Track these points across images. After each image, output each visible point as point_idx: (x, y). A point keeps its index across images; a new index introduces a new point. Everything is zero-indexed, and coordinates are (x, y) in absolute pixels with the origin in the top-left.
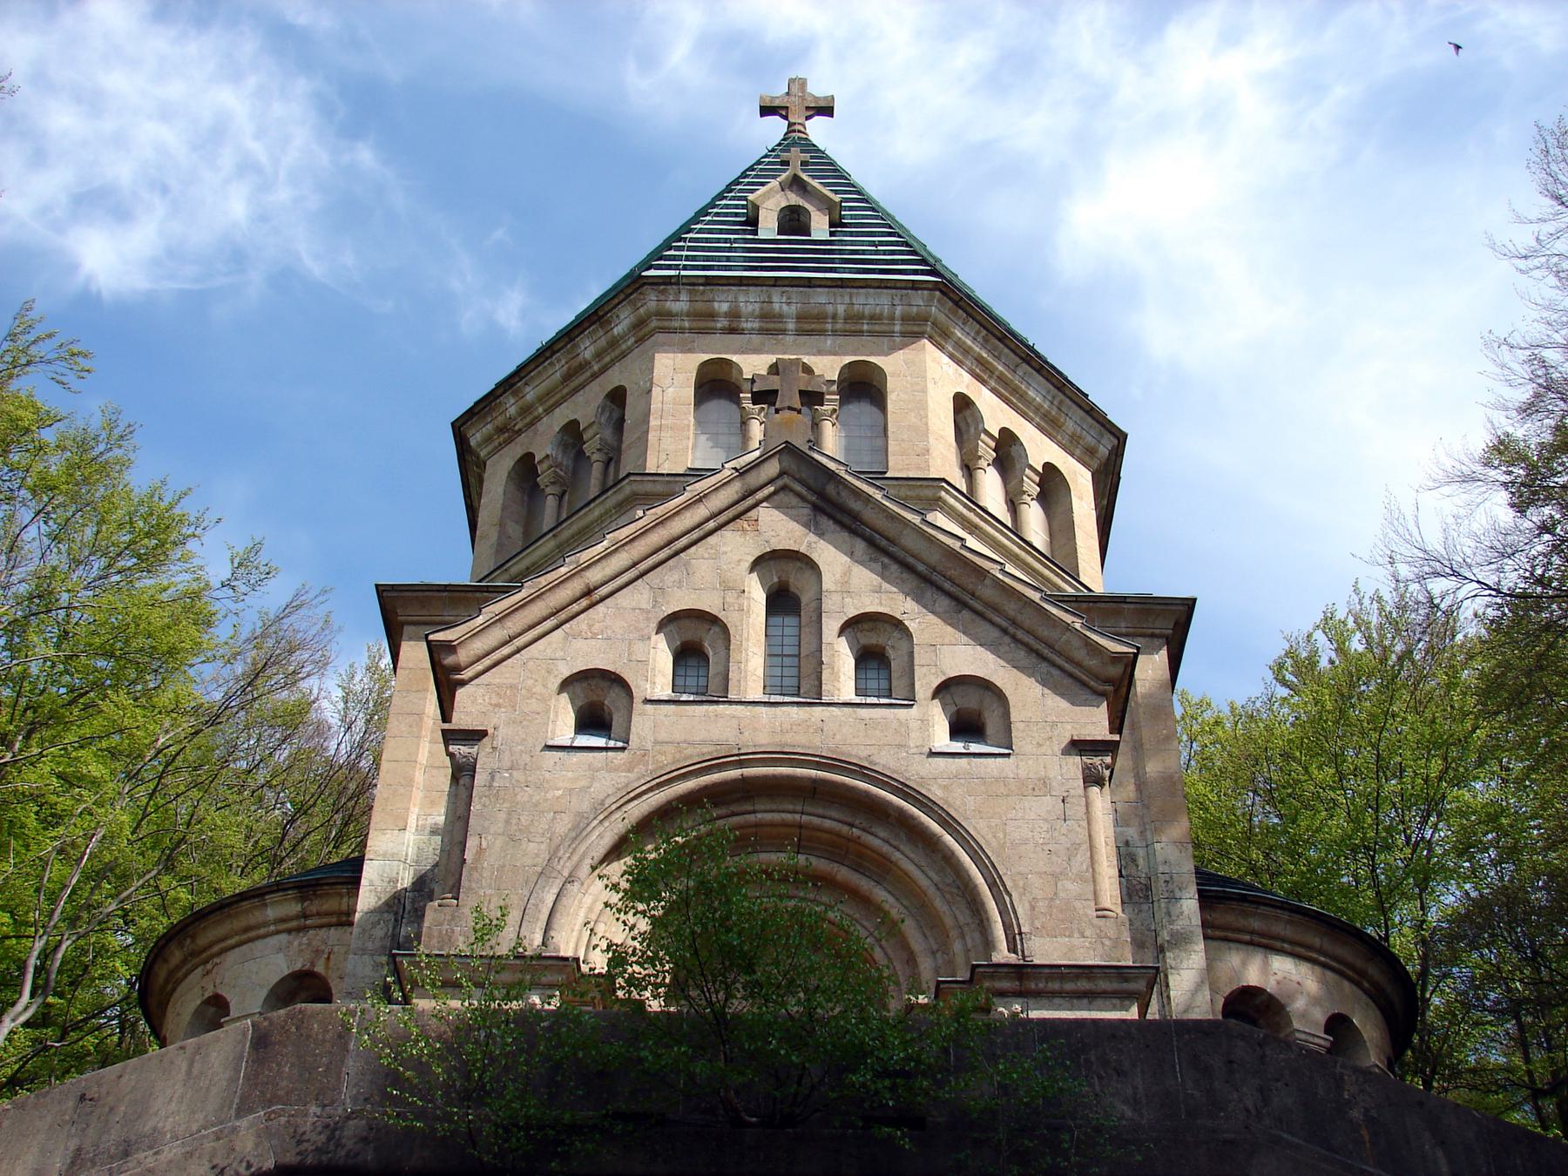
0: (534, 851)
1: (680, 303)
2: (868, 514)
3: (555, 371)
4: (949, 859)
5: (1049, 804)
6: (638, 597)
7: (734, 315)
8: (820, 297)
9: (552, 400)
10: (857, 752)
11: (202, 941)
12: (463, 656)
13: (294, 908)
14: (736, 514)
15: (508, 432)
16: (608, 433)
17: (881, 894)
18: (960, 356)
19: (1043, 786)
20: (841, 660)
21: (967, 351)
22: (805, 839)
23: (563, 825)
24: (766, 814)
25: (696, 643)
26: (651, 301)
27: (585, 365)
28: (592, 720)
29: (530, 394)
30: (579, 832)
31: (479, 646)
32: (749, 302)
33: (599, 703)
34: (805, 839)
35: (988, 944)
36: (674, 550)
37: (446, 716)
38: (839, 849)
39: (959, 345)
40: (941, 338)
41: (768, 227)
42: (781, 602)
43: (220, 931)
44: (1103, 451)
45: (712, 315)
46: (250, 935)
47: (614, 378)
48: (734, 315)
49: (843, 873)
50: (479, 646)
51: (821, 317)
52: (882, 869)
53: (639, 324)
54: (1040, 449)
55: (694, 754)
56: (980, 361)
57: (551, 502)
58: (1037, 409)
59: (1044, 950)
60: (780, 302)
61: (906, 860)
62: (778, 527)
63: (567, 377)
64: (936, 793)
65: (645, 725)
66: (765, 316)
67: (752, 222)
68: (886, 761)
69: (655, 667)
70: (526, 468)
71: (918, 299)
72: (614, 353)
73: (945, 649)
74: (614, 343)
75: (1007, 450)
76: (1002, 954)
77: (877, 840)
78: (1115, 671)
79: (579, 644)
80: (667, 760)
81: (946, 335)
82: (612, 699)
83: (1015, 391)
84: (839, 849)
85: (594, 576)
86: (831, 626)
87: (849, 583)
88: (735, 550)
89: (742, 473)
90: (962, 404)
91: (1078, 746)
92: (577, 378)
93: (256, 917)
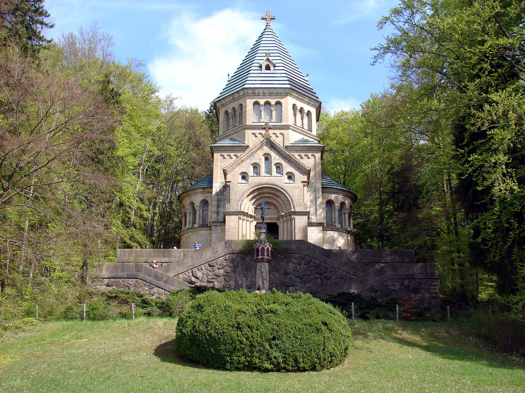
0: (238, 197)
1: (250, 91)
2: (277, 148)
3: (231, 98)
4: (287, 197)
5: (299, 190)
6: (248, 161)
7: (259, 93)
8: (272, 90)
9: (230, 102)
10: (276, 183)
11: (189, 193)
12: (227, 171)
13: (202, 191)
14: (260, 148)
15: (223, 105)
16: (240, 110)
17: (279, 200)
18: (294, 97)
19: (298, 187)
20: (274, 168)
21: (295, 96)
22: (269, 193)
23: (241, 194)
24: (265, 191)
25: (256, 166)
26: (246, 91)
27: (235, 98)
28: (244, 178)
29: (227, 100)
30: (243, 194)
31: (229, 169)
32: (261, 91)
33: (244, 176)
34: (269, 193)
35: (291, 208)
36: (253, 154)
37: (225, 179)
38: (274, 194)
39: (294, 96)
40: (291, 95)
41: (264, 68)
42: (267, 159)
43: (192, 192)
44: (318, 106)
45: (255, 93)
46: (196, 193)
47: (241, 101)
48: (259, 93)
49: (275, 197)
50: (229, 169)
51: (272, 93)
52: (279, 197)
53: (244, 94)
54: (307, 108)
55: (257, 183)
56: (297, 97)
57: (231, 120)
58: (307, 102)
59: (298, 209)
60: (265, 91)
61: (282, 196)
62: (266, 149)
63: (233, 99)
64: (285, 189)
65: (250, 179)
66: (263, 93)
67: (261, 67)
68: (279, 184)
69: (251, 171)
70: (227, 112)
71: (287, 90)
72: (240, 97)
73: (288, 168)
74: (240, 96)
75: (301, 110)
76: (293, 210)
77: (278, 194)
78: (308, 172)
79: (241, 168)
80: (253, 184)
81: (292, 95)
82: (246, 175)
83: (303, 100)
84: (274, 194)
85: (243, 159)
86: (273, 164)
87: (275, 158)
88: (261, 153)
89: (261, 142)
90: (294, 106)
91: (303, 182)
92: (234, 100)
93: (197, 191)
